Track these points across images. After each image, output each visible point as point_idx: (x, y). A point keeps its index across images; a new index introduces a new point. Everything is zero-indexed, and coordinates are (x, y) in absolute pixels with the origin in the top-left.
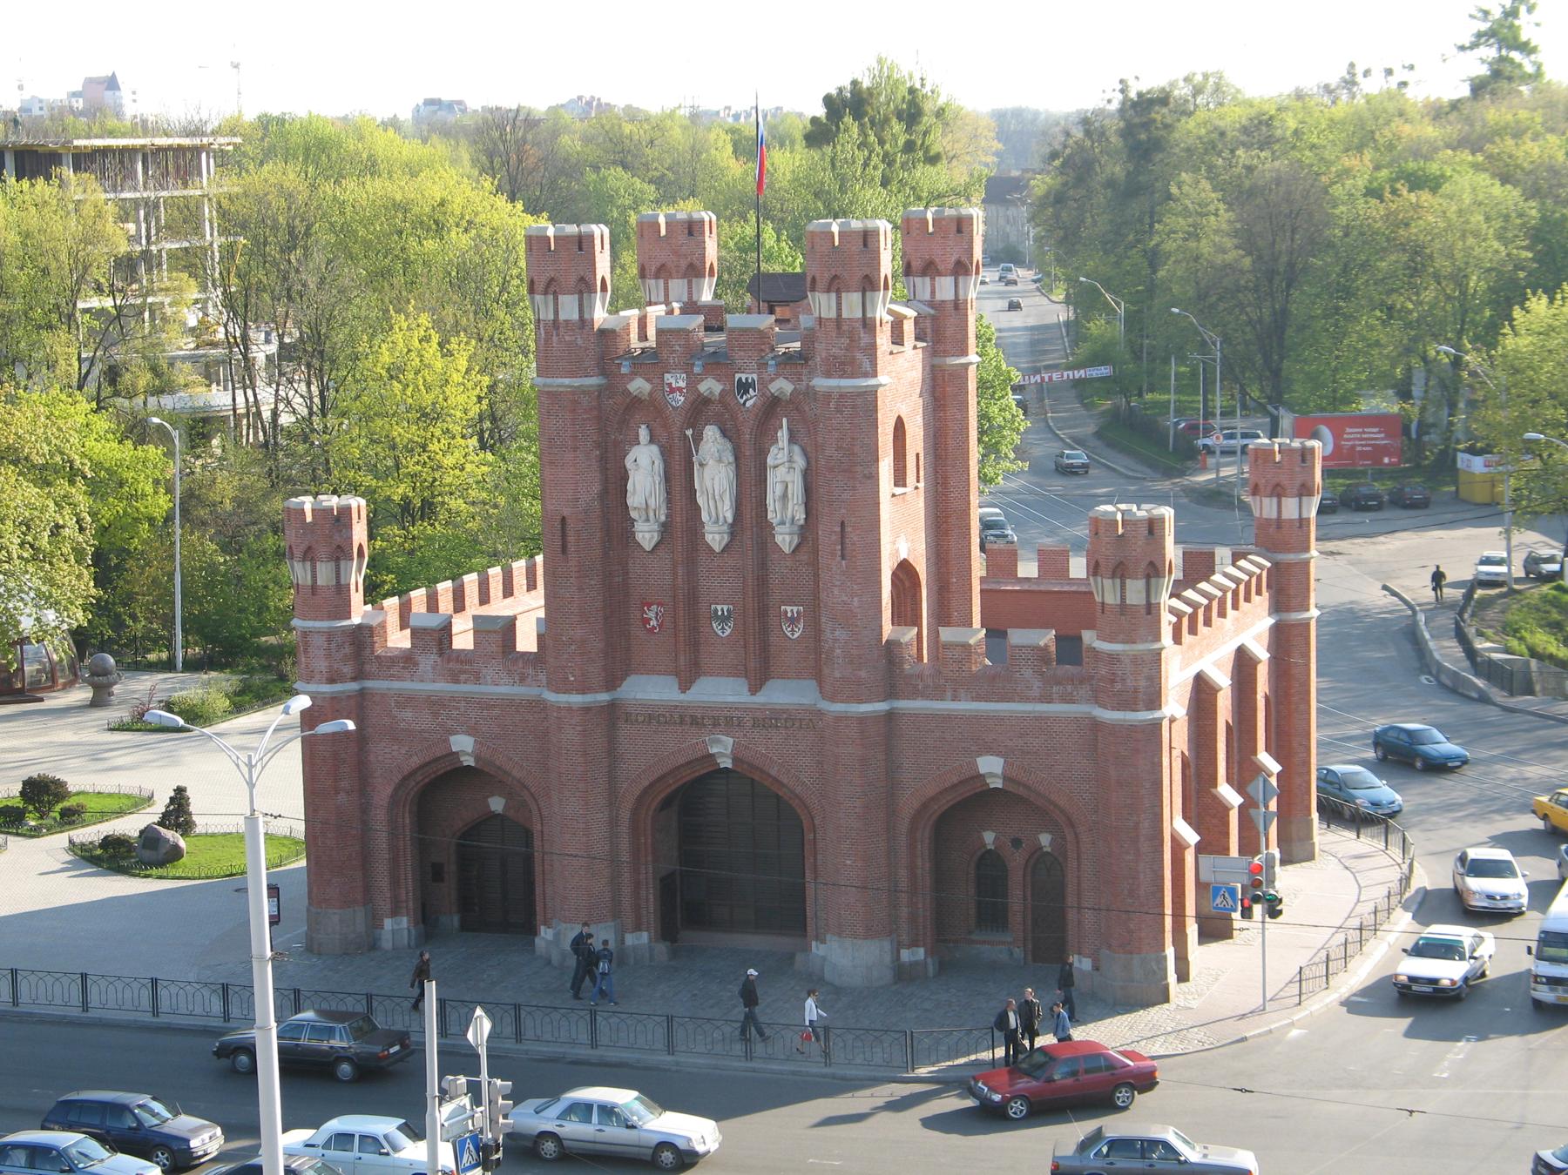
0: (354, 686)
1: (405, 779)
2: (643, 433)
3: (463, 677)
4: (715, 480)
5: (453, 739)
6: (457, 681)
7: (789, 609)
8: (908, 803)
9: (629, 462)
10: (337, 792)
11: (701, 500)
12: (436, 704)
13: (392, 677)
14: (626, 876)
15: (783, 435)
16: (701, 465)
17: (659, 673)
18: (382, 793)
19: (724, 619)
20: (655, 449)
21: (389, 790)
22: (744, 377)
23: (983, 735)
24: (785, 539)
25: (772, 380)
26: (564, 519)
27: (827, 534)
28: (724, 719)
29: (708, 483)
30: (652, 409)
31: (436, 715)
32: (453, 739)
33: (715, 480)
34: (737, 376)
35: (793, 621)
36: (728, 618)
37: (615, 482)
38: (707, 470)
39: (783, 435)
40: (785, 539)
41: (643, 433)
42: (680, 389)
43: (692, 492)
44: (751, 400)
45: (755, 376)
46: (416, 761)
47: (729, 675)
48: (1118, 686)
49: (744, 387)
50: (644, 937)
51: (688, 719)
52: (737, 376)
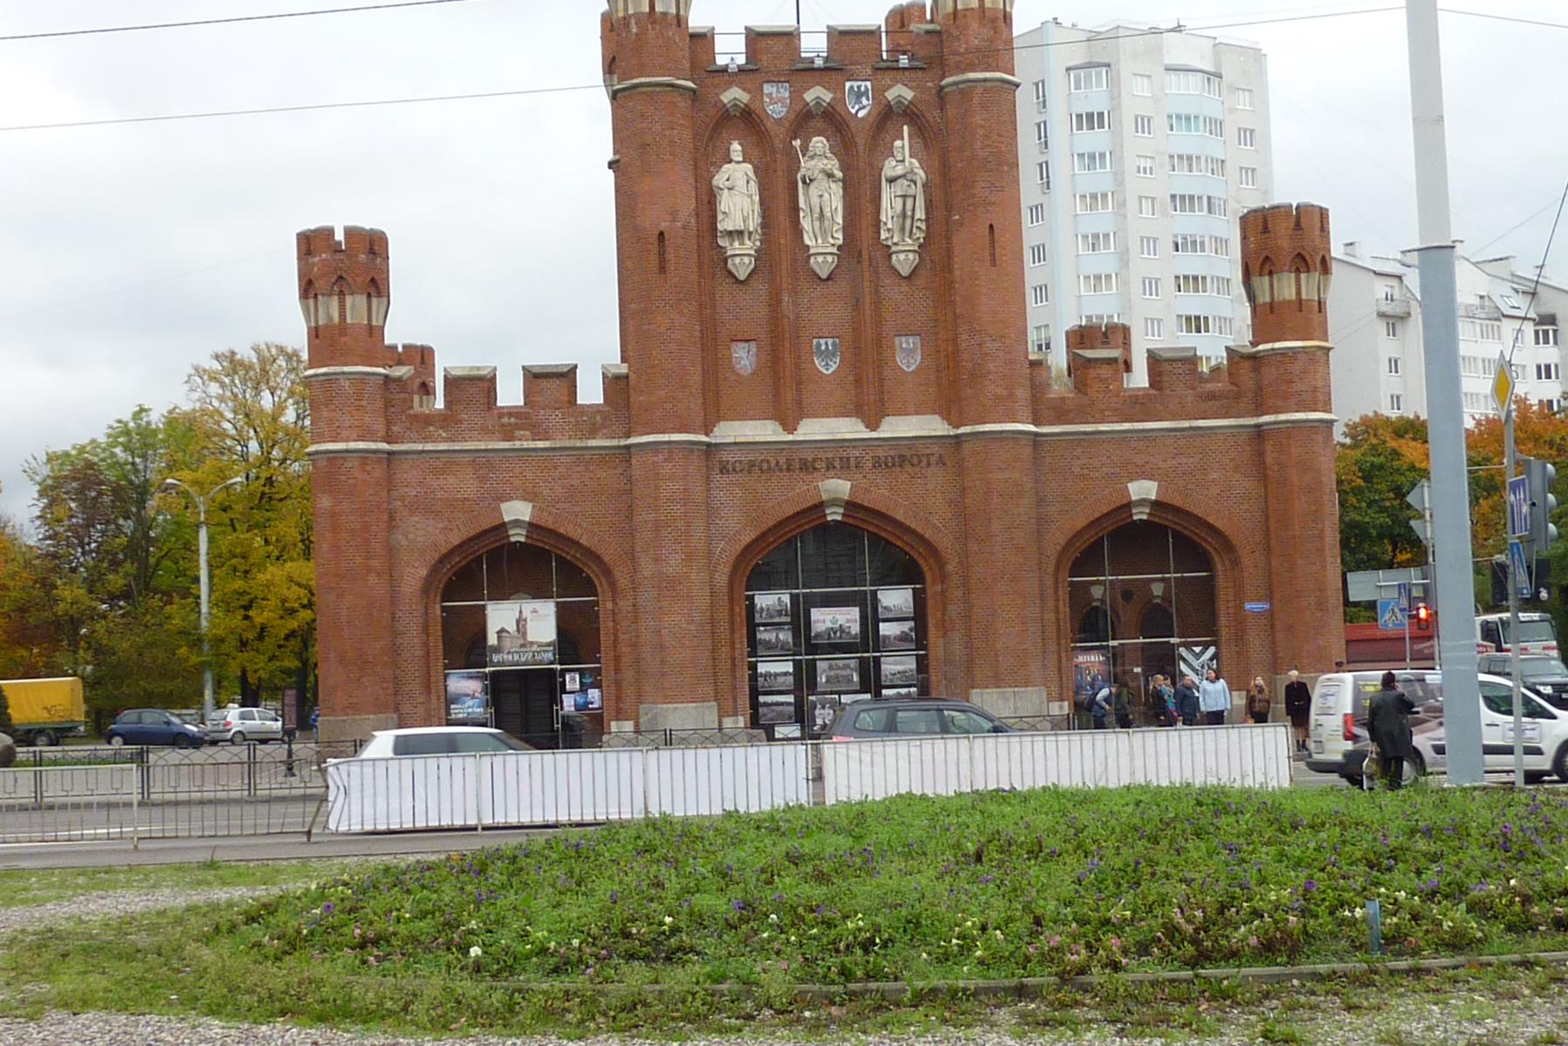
0: (384, 446)
3: (518, 433)
5: (504, 506)
6: (509, 437)
7: (903, 339)
8: (1057, 537)
9: (719, 180)
10: (369, 571)
11: (806, 223)
12: (482, 463)
13: (426, 439)
14: (724, 652)
15: (903, 145)
16: (804, 182)
18: (414, 575)
19: (827, 355)
20: (748, 167)
21: (423, 572)
22: (855, 84)
23: (1135, 455)
24: (904, 261)
25: (890, 87)
26: (661, 234)
27: (967, 245)
28: (837, 457)
29: (815, 201)
30: (748, 120)
31: (482, 479)
32: (504, 506)
33: (823, 200)
34: (848, 84)
35: (910, 352)
36: (834, 355)
37: (708, 201)
39: (903, 145)
40: (904, 261)
41: (736, 147)
42: (781, 100)
43: (795, 209)
44: (861, 110)
45: (869, 84)
46: (456, 540)
48: (1298, 386)
49: (859, 95)
50: (741, 721)
52: (848, 84)
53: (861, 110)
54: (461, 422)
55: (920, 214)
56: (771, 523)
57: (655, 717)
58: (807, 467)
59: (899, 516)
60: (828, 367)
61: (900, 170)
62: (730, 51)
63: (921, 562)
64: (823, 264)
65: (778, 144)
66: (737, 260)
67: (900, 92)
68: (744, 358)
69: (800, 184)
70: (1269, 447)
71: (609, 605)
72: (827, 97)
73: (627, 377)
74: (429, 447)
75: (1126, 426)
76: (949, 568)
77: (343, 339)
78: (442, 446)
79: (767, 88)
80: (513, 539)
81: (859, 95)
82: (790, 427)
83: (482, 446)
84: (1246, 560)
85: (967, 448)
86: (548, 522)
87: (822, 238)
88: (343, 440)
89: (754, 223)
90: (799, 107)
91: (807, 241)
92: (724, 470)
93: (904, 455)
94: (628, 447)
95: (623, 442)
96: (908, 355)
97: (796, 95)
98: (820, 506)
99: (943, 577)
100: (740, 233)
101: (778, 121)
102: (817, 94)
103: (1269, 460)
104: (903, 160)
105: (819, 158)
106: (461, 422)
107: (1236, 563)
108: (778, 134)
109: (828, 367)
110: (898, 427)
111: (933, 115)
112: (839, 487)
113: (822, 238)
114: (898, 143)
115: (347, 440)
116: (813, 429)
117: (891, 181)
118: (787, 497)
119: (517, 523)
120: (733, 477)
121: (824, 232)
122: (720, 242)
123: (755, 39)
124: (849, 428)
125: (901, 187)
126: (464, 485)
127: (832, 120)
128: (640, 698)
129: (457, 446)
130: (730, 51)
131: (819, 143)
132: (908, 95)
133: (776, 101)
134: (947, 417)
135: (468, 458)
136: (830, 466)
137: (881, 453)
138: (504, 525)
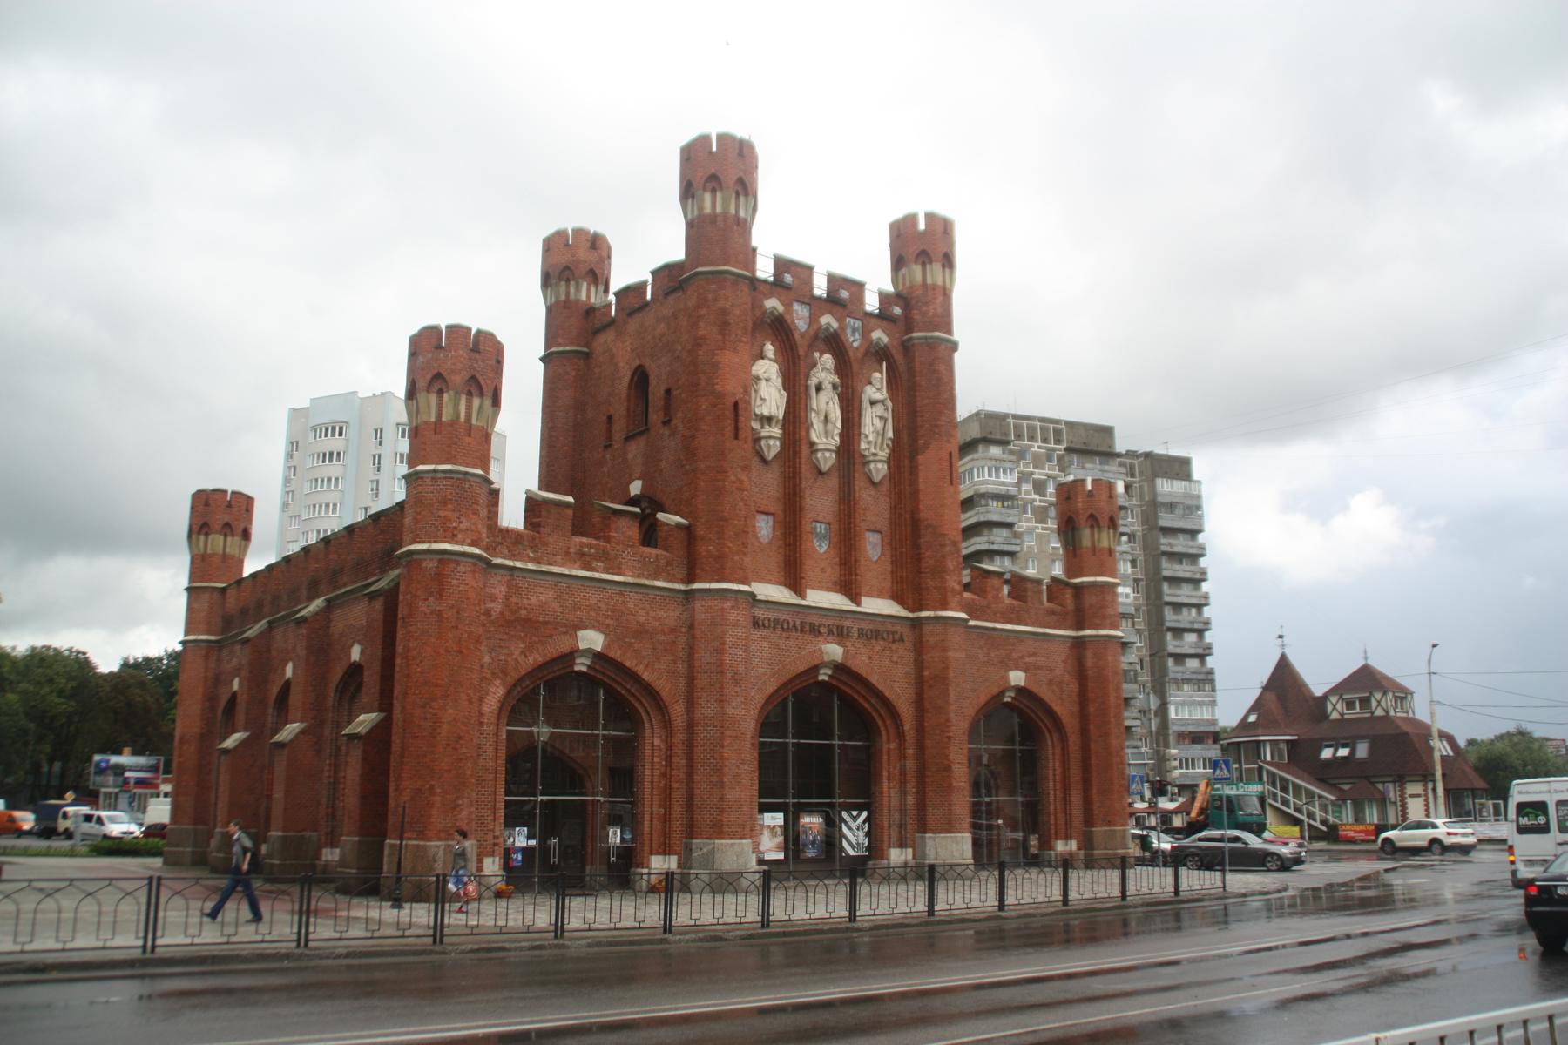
1: (522, 679)
2: (769, 349)
3: (594, 564)
4: (825, 405)
13: (513, 557)
17: (770, 582)
19: (821, 537)
29: (823, 406)
30: (779, 328)
32: (580, 634)
33: (825, 405)
38: (823, 394)
39: (880, 377)
40: (879, 470)
43: (807, 408)
47: (828, 589)
51: (807, 628)
53: (854, 340)
54: (546, 544)
55: (890, 434)
56: (788, 677)
57: (712, 852)
58: (815, 630)
59: (874, 680)
61: (878, 396)
62: (764, 269)
63: (880, 722)
64: (827, 460)
65: (801, 352)
66: (771, 442)
67: (879, 335)
68: (764, 528)
69: (813, 390)
70: (1089, 653)
71: (657, 741)
72: (835, 325)
73: (688, 530)
74: (518, 564)
75: (1009, 627)
76: (907, 727)
77: (468, 440)
78: (530, 566)
79: (796, 306)
80: (577, 668)
81: (854, 330)
82: (798, 590)
83: (566, 571)
84: (1071, 741)
85: (927, 629)
86: (616, 654)
88: (457, 543)
90: (815, 327)
91: (814, 437)
92: (756, 623)
93: (876, 629)
94: (686, 592)
95: (682, 587)
97: (813, 319)
98: (815, 669)
99: (901, 736)
100: (769, 420)
101: (803, 335)
102: (827, 320)
103: (1089, 662)
104: (875, 389)
106: (546, 544)
107: (1064, 740)
111: (899, 357)
112: (834, 651)
114: (877, 375)
115: (462, 543)
117: (873, 403)
119: (588, 652)
120: (764, 632)
121: (827, 434)
122: (756, 425)
123: (782, 265)
124: (837, 601)
125: (879, 410)
127: (834, 343)
128: (691, 832)
129: (544, 568)
130: (764, 269)
131: (828, 360)
132: (885, 339)
133: (800, 317)
134: (901, 601)
135: (550, 580)
136: (830, 632)
137: (864, 625)
138: (573, 653)
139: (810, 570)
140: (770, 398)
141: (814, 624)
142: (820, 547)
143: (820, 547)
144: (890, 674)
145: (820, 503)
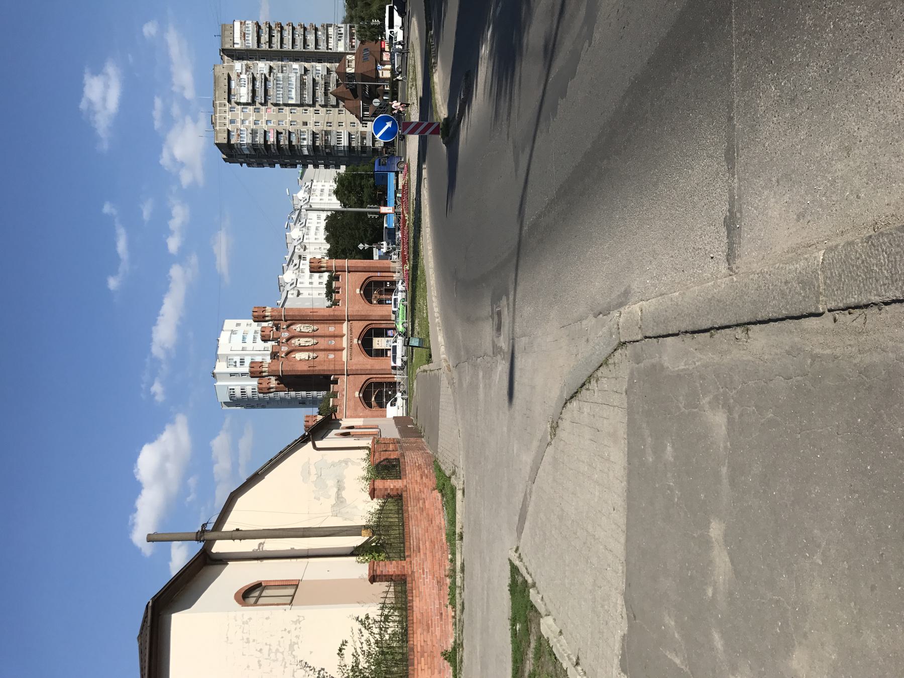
4: (303, 341)
28: (351, 340)
60: (333, 342)
68: (331, 356)
87: (310, 342)
89: (307, 353)
93: (351, 330)
96: (332, 329)
105: (295, 342)
108: (291, 349)
109: (333, 342)
110: (345, 331)
112: (355, 341)
113: (310, 342)
116: (345, 345)
118: (357, 349)
124: (345, 338)
126: (352, 403)
131: (293, 341)
139: (338, 347)
140: (303, 355)
141: (351, 346)
142: (332, 342)
143: (332, 342)
144: (359, 326)
145: (323, 343)
